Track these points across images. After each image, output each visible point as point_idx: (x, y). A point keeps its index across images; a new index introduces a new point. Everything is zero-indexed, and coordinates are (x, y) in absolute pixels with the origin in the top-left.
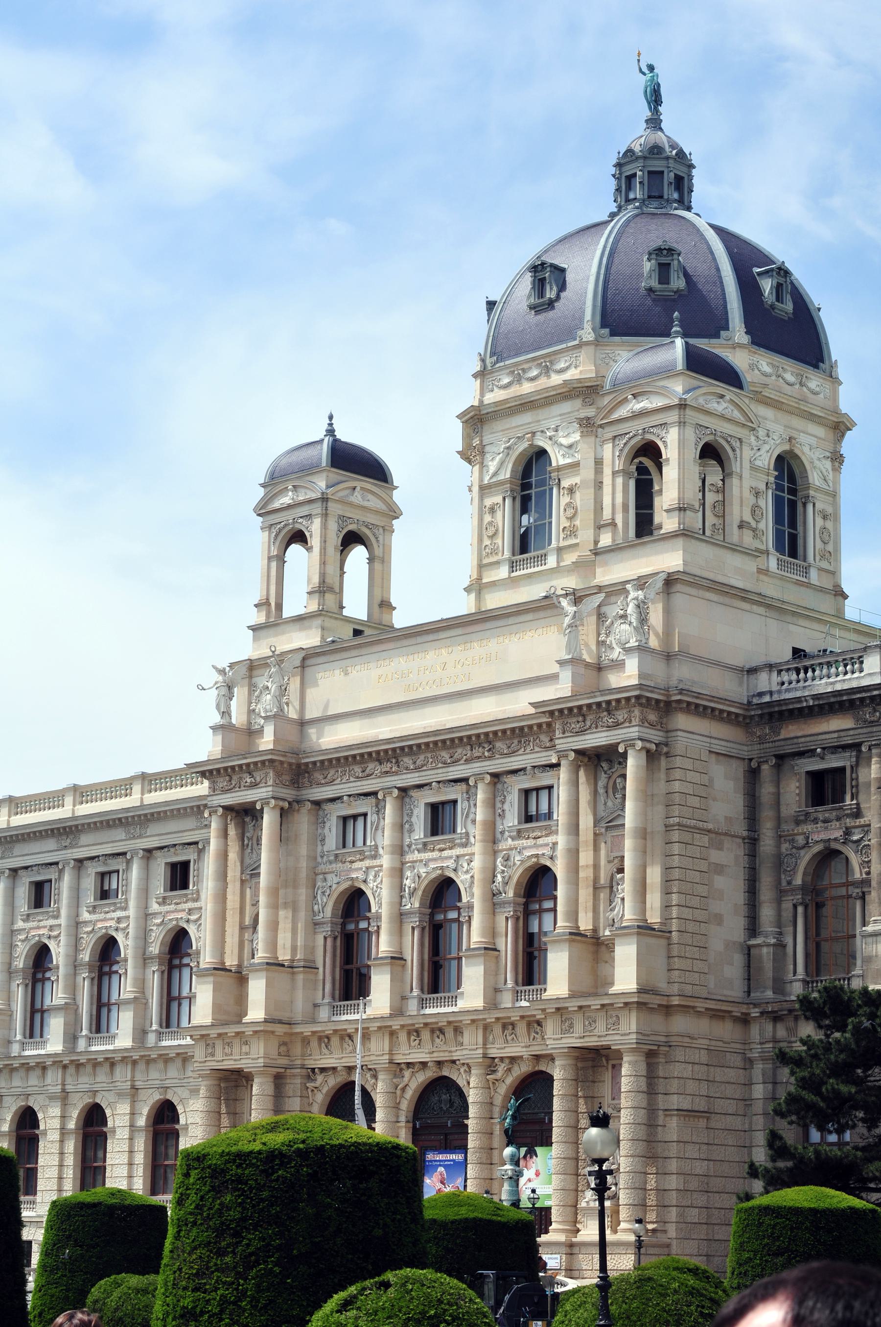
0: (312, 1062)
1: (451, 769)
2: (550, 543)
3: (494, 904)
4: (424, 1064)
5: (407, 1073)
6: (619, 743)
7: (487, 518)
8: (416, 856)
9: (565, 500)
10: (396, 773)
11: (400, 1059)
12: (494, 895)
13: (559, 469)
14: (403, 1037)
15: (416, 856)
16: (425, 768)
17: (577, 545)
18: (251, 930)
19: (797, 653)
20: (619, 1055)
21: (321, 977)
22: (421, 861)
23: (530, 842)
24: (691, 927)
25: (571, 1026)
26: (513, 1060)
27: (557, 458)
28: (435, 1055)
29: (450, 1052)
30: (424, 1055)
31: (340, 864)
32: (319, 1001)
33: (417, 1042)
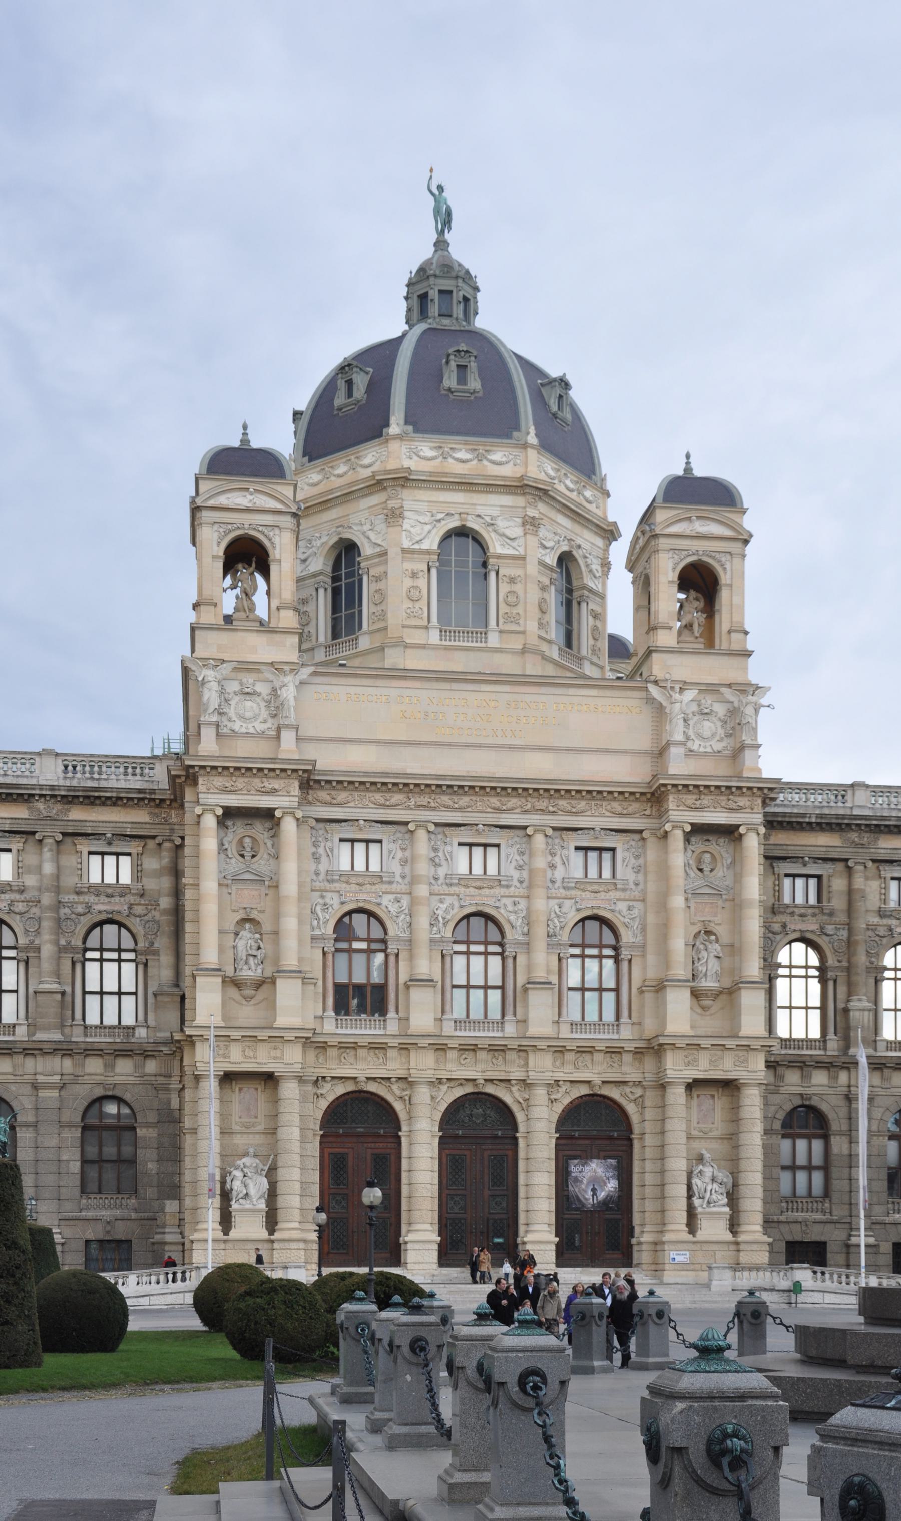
0: (325, 1070)
1: (503, 816)
3: (548, 945)
5: (444, 1088)
7: (408, 582)
8: (446, 889)
11: (444, 1075)
12: (548, 936)
14: (452, 1054)
15: (446, 889)
16: (469, 809)
18: (232, 935)
21: (321, 990)
22: (458, 896)
23: (588, 895)
25: (696, 1060)
27: (496, 546)
28: (488, 1073)
29: (509, 1072)
30: (475, 1073)
31: (344, 885)
32: (320, 1013)
33: (468, 1060)
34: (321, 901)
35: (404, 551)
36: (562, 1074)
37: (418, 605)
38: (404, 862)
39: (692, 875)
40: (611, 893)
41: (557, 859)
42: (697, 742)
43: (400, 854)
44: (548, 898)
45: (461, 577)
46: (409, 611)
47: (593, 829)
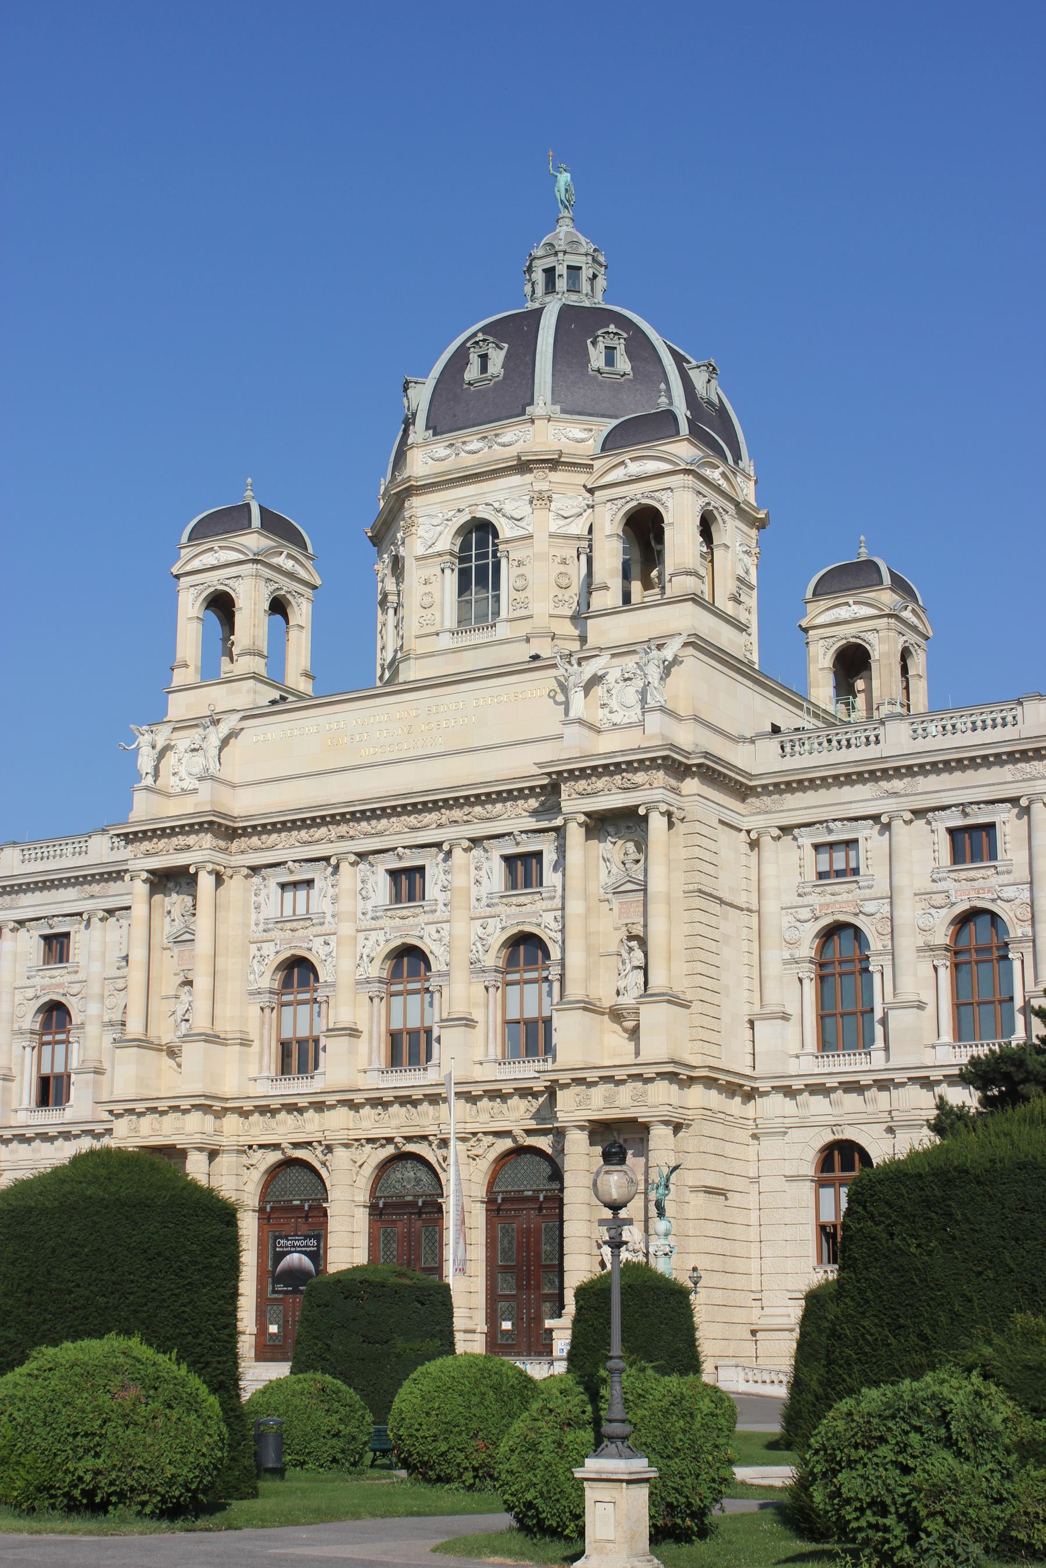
2: (497, 613)
4: (390, 1140)
6: (639, 805)
9: (516, 571)
10: (352, 838)
12: (472, 963)
13: (507, 542)
15: (374, 924)
17: (531, 617)
19: (776, 730)
20: (646, 1128)
24: (707, 996)
26: (498, 1134)
27: (506, 530)
34: (258, 954)
35: (418, 559)
36: (477, 1125)
37: (429, 611)
38: (335, 900)
39: (614, 870)
40: (538, 903)
41: (483, 873)
42: (621, 713)
43: (331, 891)
44: (472, 919)
45: (482, 570)
46: (421, 620)
47: (510, 834)
